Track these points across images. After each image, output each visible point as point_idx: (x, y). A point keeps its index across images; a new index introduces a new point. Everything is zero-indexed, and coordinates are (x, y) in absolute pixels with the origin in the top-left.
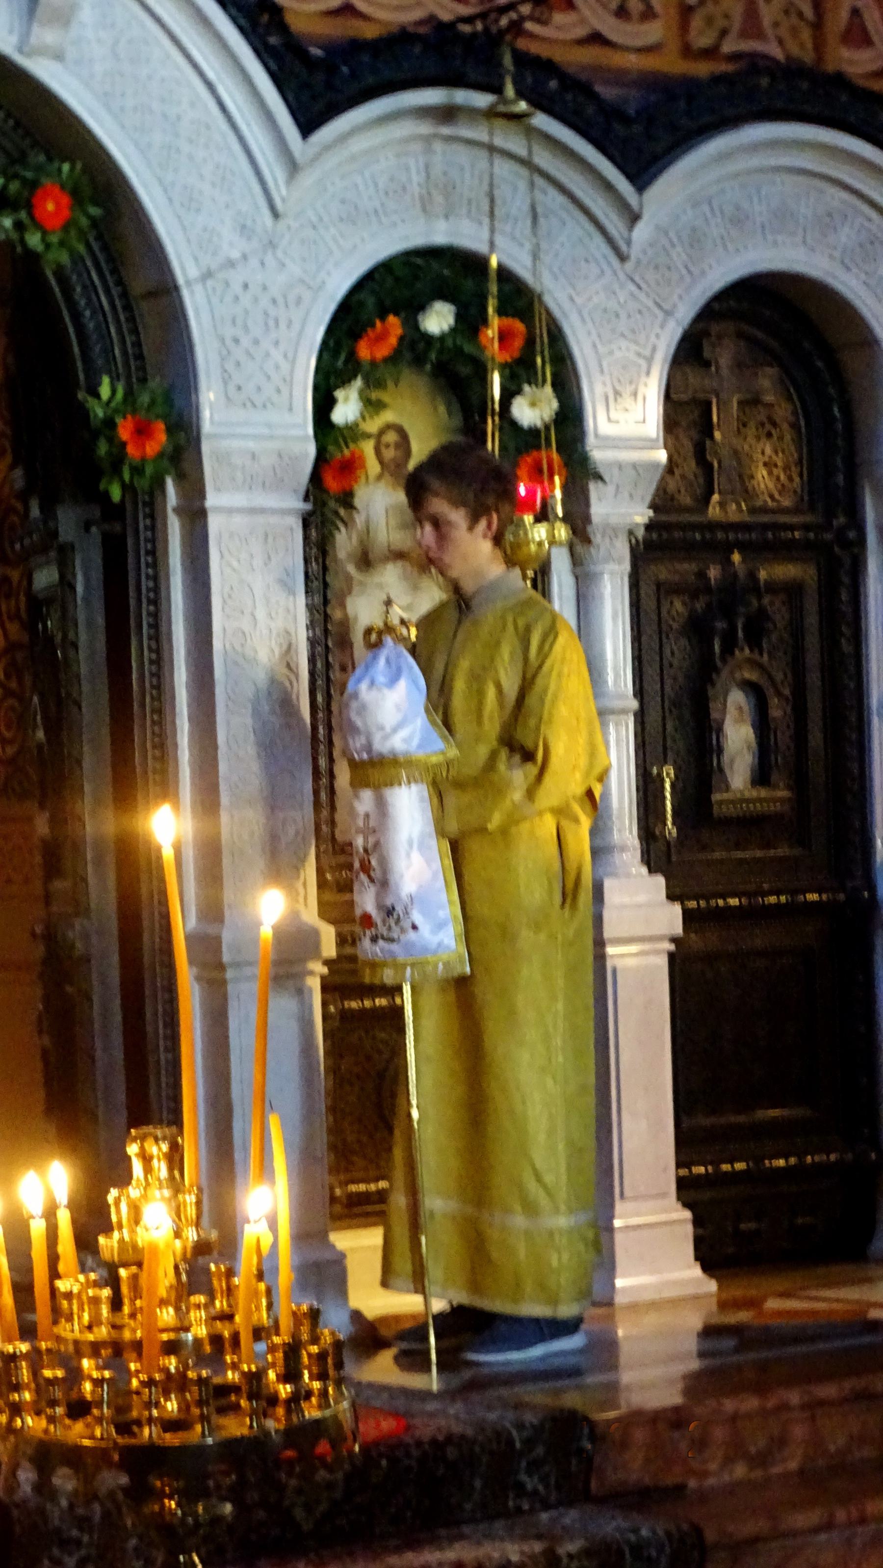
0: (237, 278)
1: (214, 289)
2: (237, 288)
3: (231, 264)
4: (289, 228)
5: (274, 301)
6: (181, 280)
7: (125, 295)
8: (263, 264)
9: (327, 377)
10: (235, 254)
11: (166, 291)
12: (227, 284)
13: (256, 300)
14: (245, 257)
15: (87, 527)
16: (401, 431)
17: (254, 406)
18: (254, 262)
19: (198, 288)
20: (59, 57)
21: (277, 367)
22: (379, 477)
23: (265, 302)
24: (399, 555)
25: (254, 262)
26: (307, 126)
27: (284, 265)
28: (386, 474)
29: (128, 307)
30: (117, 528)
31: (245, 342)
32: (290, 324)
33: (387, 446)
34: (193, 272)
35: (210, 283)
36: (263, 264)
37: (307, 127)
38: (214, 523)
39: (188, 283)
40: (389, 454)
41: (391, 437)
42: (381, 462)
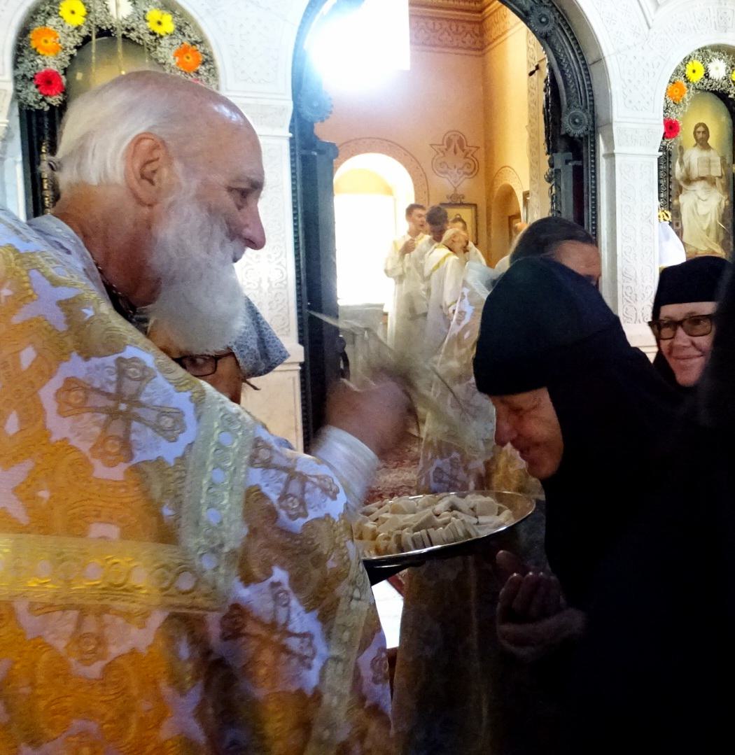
1: (621, 58)
4: (655, 33)
5: (647, 64)
6: (605, 54)
7: (585, 64)
11: (600, 60)
15: (567, 162)
16: (704, 126)
17: (637, 109)
21: (648, 93)
22: (696, 145)
24: (703, 178)
28: (698, 145)
29: (586, 69)
30: (579, 163)
33: (699, 132)
36: (643, 48)
38: (618, 159)
39: (609, 55)
40: (700, 136)
41: (701, 129)
42: (697, 140)
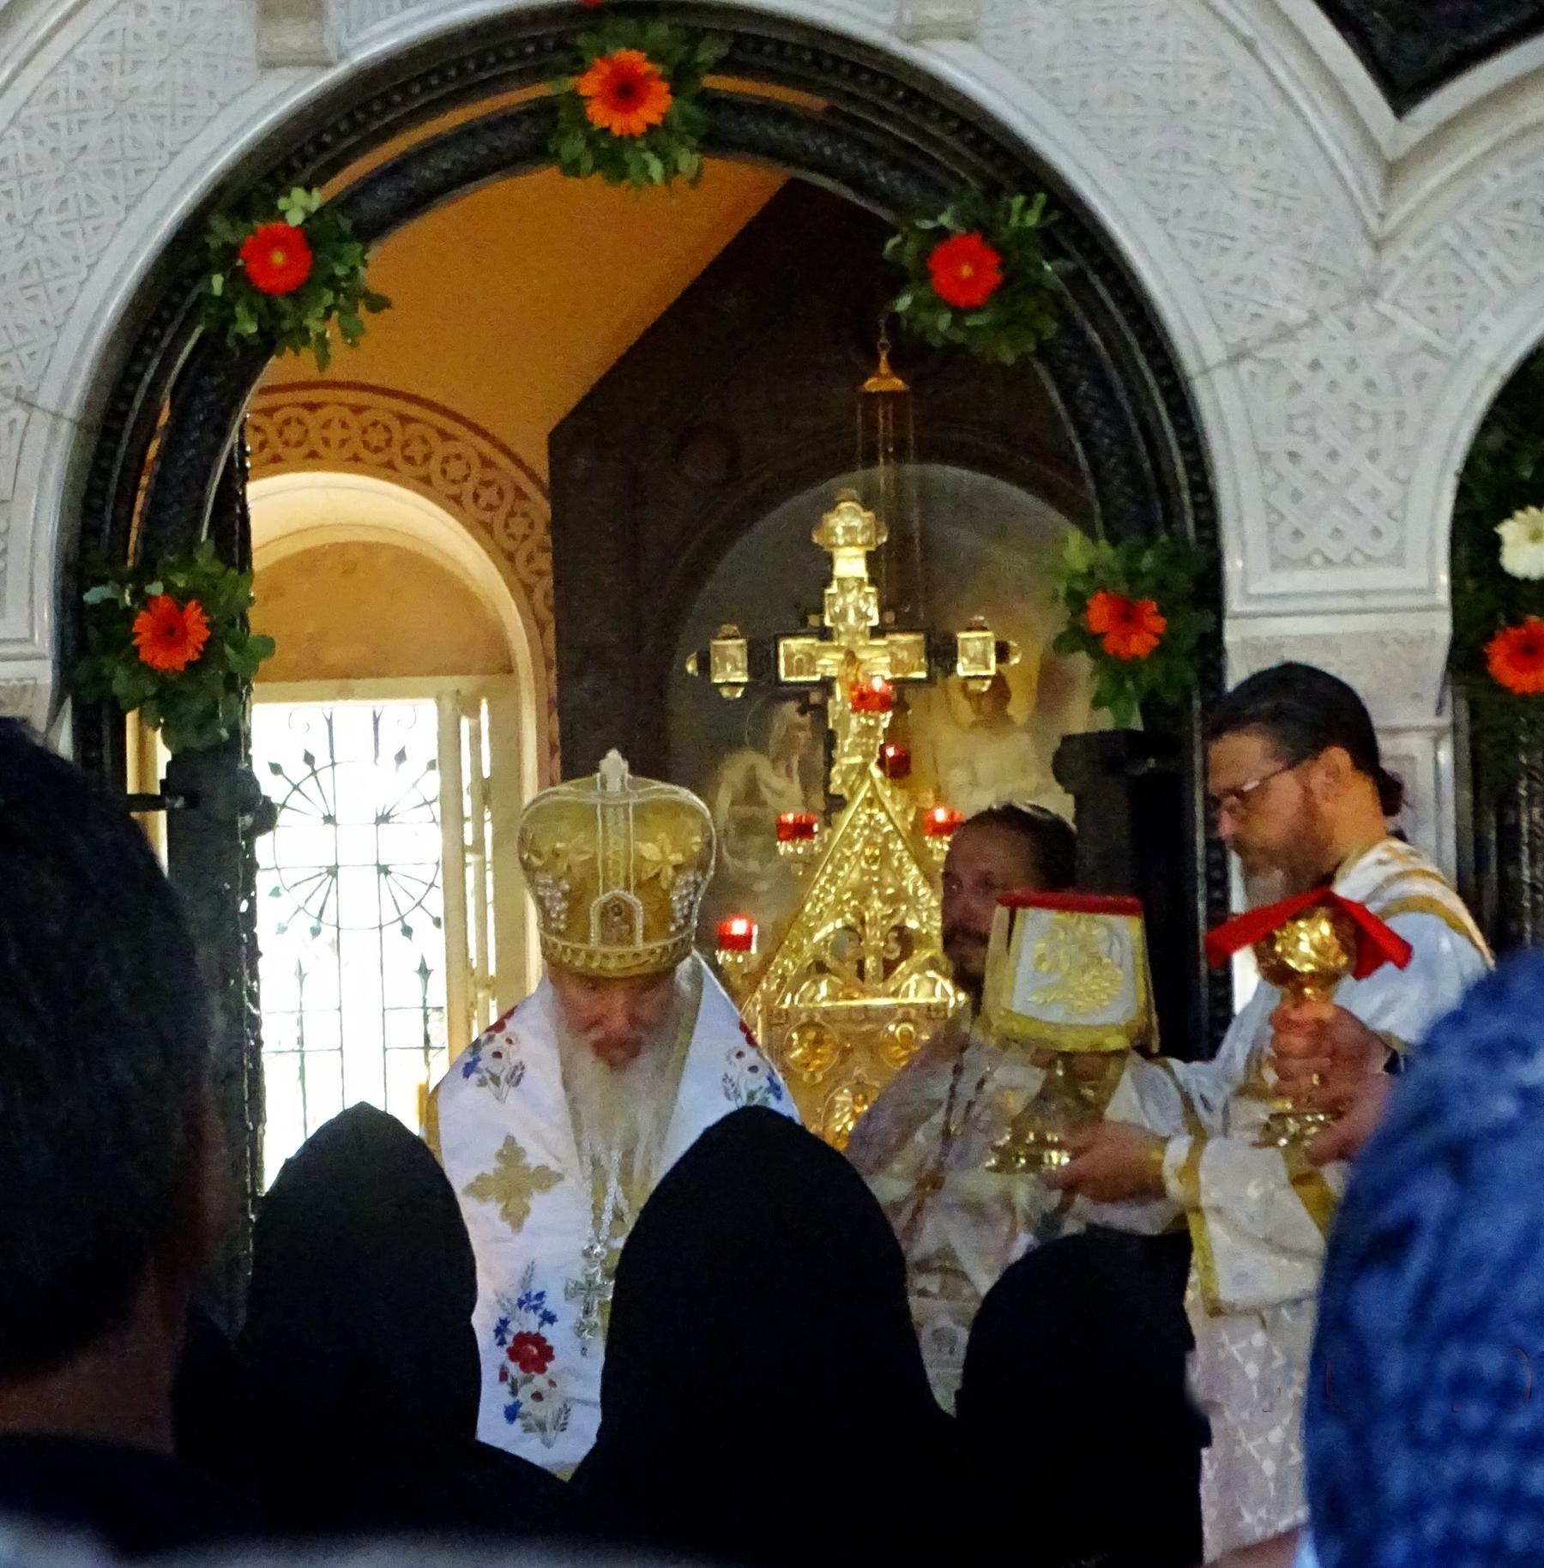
0: (1297, 355)
1: (1253, 374)
2: (1300, 372)
3: (1285, 332)
4: (1405, 260)
5: (1370, 385)
8: (1350, 326)
9: (1480, 499)
10: (1296, 315)
12: (1276, 365)
13: (1333, 386)
14: (1314, 319)
18: (1331, 324)
19: (1221, 377)
20: (967, 36)
23: (1352, 386)
25: (1331, 324)
26: (1404, 91)
27: (1393, 323)
31: (1313, 456)
32: (1401, 419)
34: (1214, 352)
35: (1246, 366)
36: (1350, 326)
37: (1404, 91)
